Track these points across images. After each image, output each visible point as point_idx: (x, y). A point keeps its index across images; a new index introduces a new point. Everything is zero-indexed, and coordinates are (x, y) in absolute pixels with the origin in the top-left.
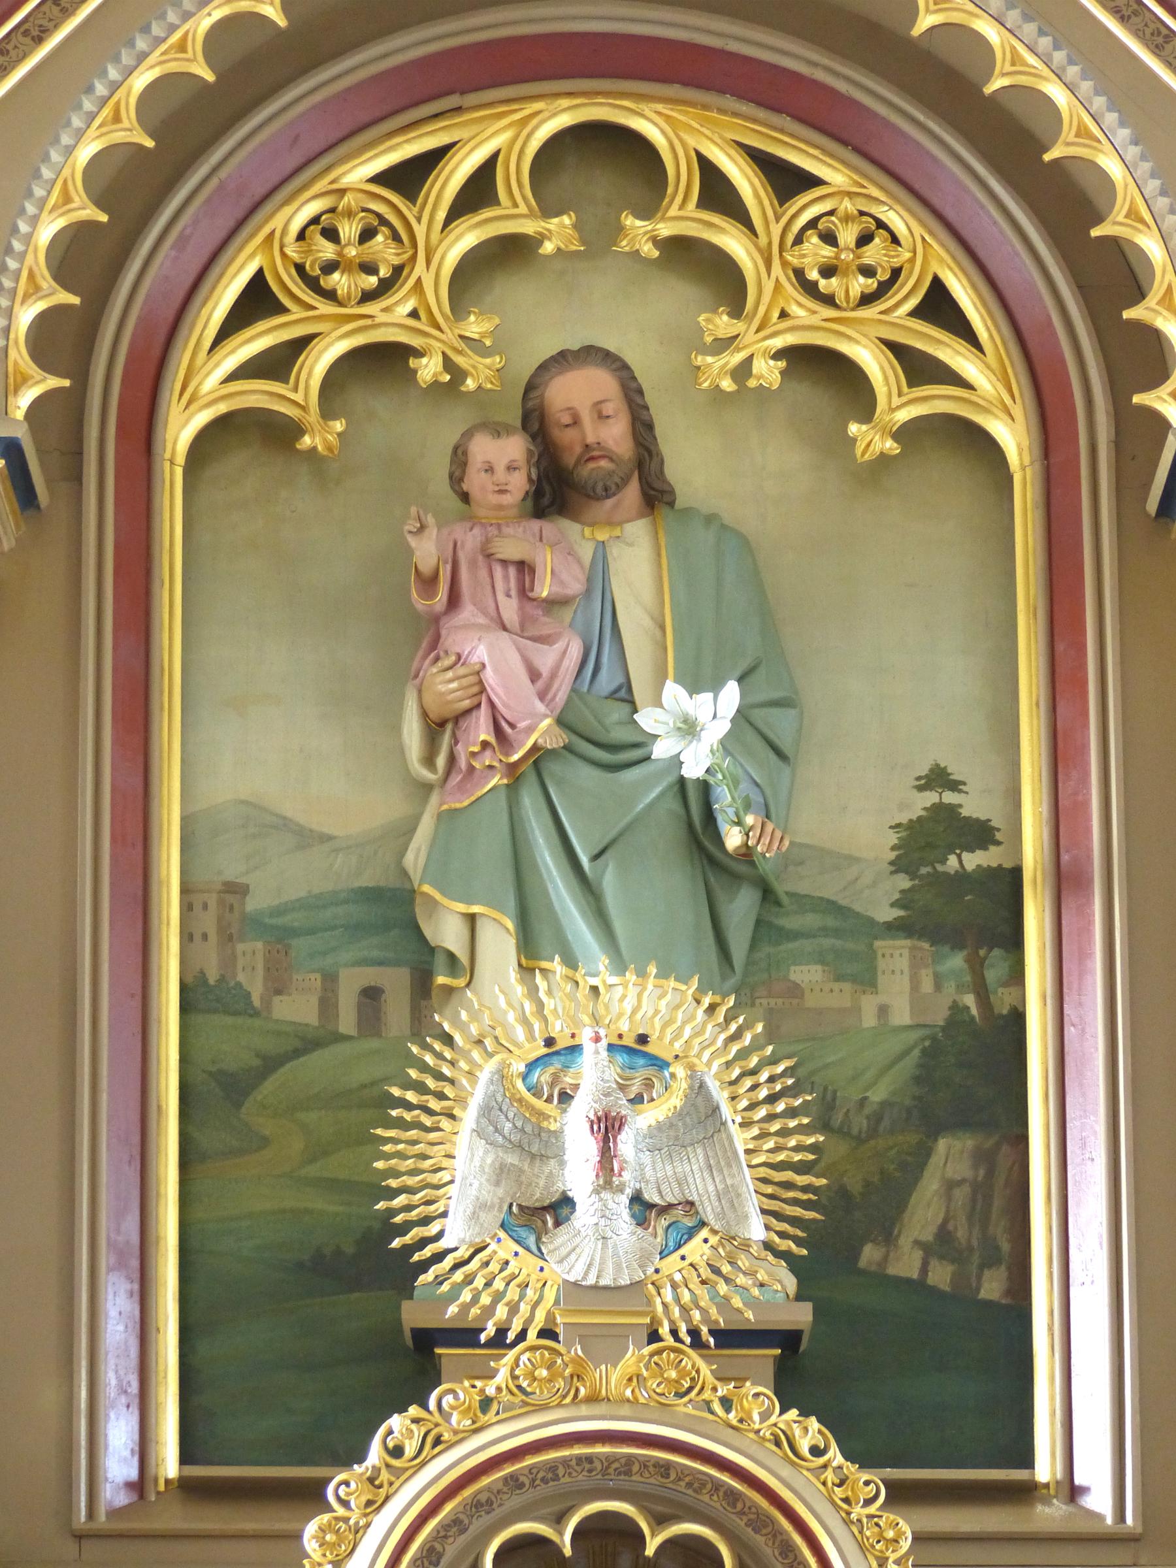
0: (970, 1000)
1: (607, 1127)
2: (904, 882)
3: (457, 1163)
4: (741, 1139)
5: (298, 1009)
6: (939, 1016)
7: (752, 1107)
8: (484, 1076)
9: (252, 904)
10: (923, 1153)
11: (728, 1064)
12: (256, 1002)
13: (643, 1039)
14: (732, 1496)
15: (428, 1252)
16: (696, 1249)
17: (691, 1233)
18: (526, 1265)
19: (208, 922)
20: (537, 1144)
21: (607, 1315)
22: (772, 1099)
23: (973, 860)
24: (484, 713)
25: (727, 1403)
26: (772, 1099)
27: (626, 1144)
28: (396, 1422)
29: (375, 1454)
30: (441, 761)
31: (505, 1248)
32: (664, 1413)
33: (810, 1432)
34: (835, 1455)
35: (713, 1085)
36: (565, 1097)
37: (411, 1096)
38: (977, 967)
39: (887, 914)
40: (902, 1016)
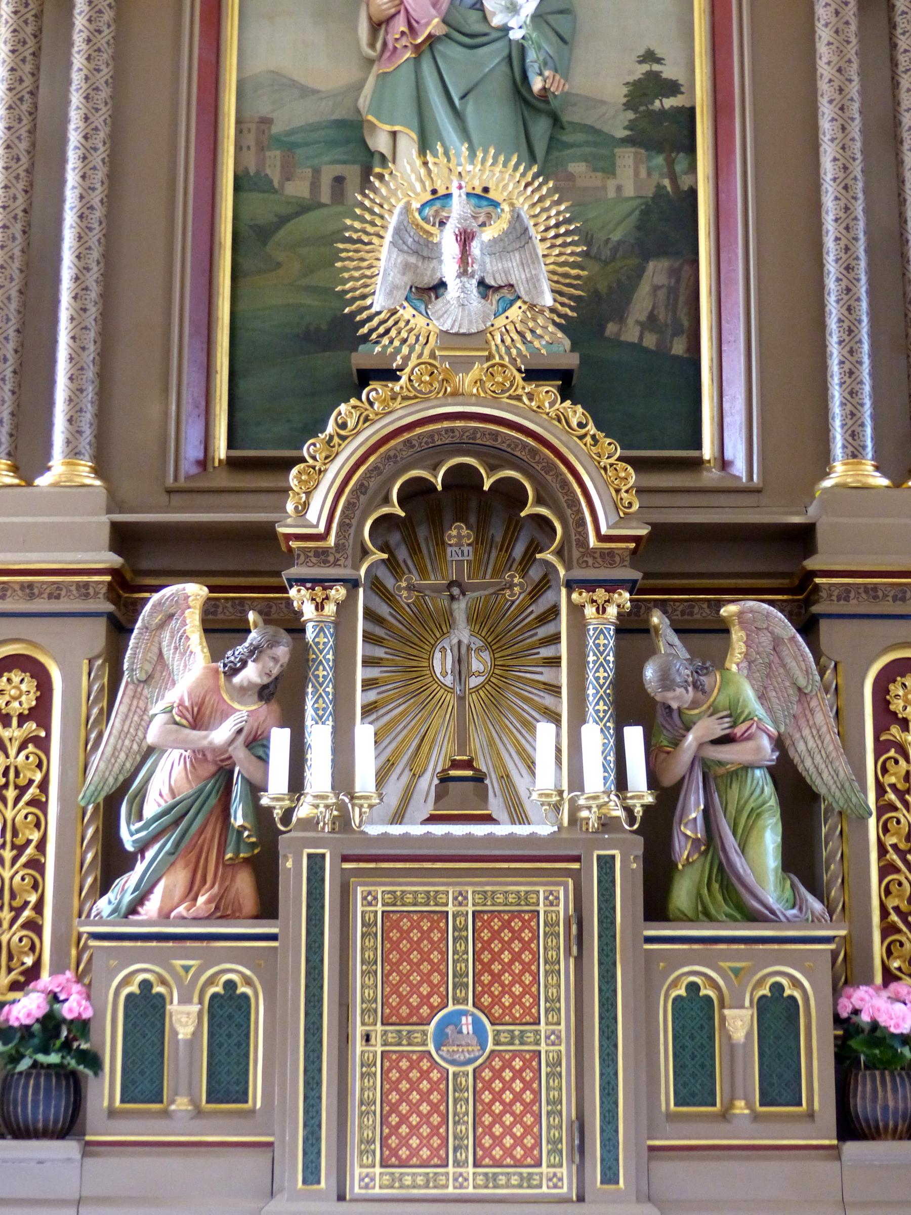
0: (666, 182)
1: (465, 238)
2: (631, 115)
3: (382, 264)
4: (541, 249)
5: (298, 189)
6: (650, 192)
7: (547, 229)
8: (397, 211)
9: (276, 129)
10: (640, 272)
11: (534, 205)
12: (276, 184)
13: (486, 190)
14: (533, 452)
15: (364, 315)
16: (515, 312)
17: (512, 303)
18: (420, 322)
19: (250, 139)
20: (426, 250)
21: (465, 344)
22: (557, 225)
23: (669, 103)
24: (401, 19)
25: (531, 396)
26: (557, 225)
27: (476, 248)
28: (343, 407)
29: (331, 428)
30: (379, 45)
31: (407, 312)
32: (494, 401)
33: (576, 414)
34: (591, 428)
35: (525, 216)
36: (442, 224)
37: (357, 225)
38: (671, 163)
39: (622, 133)
40: (629, 191)
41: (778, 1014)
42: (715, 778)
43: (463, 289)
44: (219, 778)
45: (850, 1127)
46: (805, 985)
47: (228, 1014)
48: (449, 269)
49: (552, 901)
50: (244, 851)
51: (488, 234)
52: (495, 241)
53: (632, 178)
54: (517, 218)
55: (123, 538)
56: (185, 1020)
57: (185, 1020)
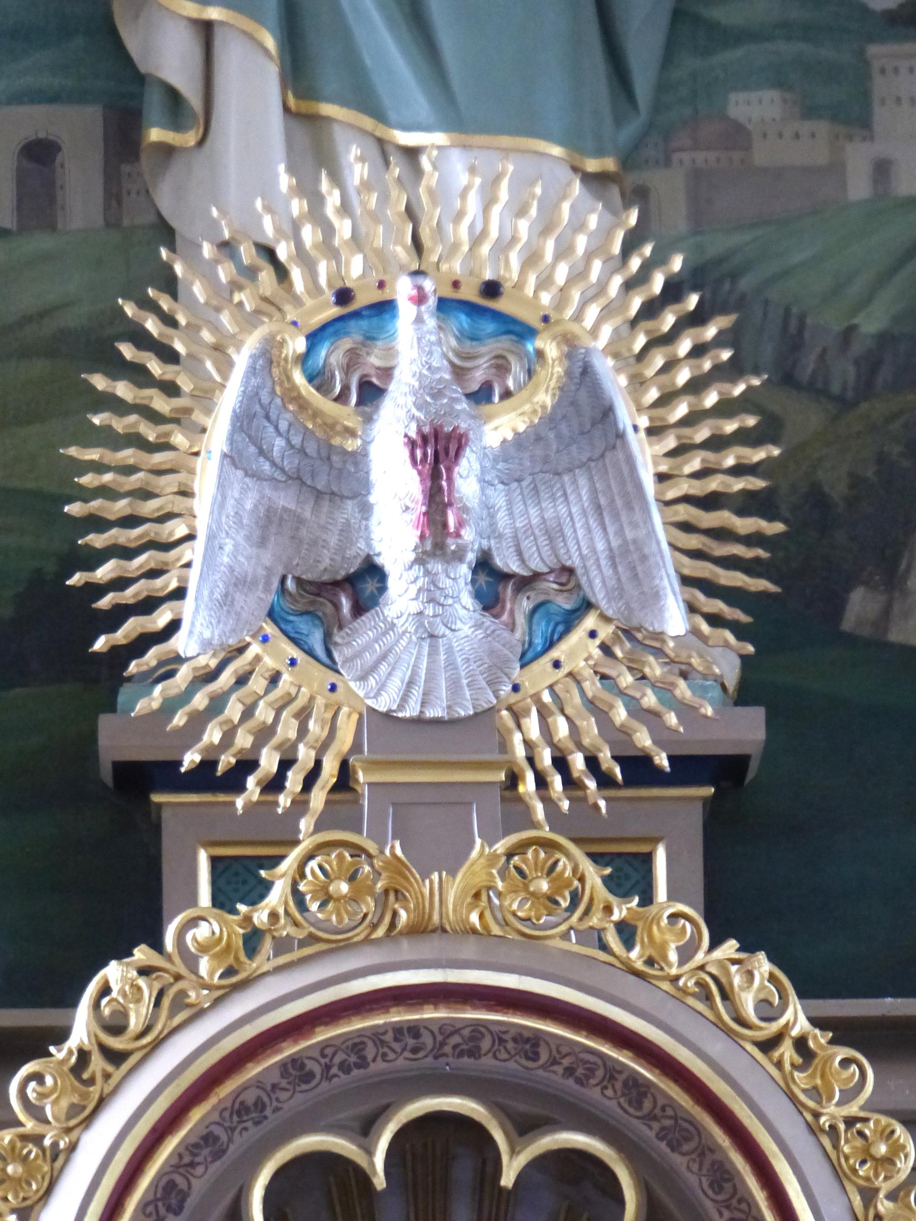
4: (647, 457)
7: (666, 399)
8: (242, 359)
16: (578, 648)
17: (570, 621)
18: (305, 680)
26: (696, 386)
31: (272, 653)
35: (604, 366)
37: (123, 390)
43: (432, 594)
48: (391, 528)
51: (500, 427)
52: (520, 441)
54: (582, 375)
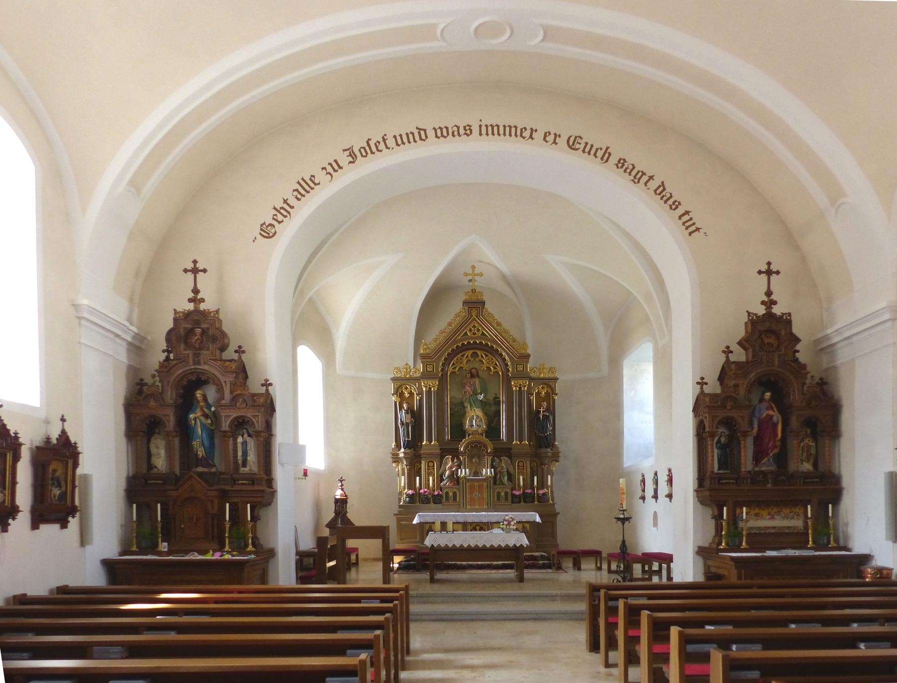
21: (475, 433)
41: (506, 493)
42: (501, 473)
44: (452, 473)
45: (513, 502)
46: (508, 490)
47: (455, 494)
49: (485, 484)
50: (455, 479)
53: (493, 408)
55: (441, 449)
56: (451, 494)
57: (451, 494)
